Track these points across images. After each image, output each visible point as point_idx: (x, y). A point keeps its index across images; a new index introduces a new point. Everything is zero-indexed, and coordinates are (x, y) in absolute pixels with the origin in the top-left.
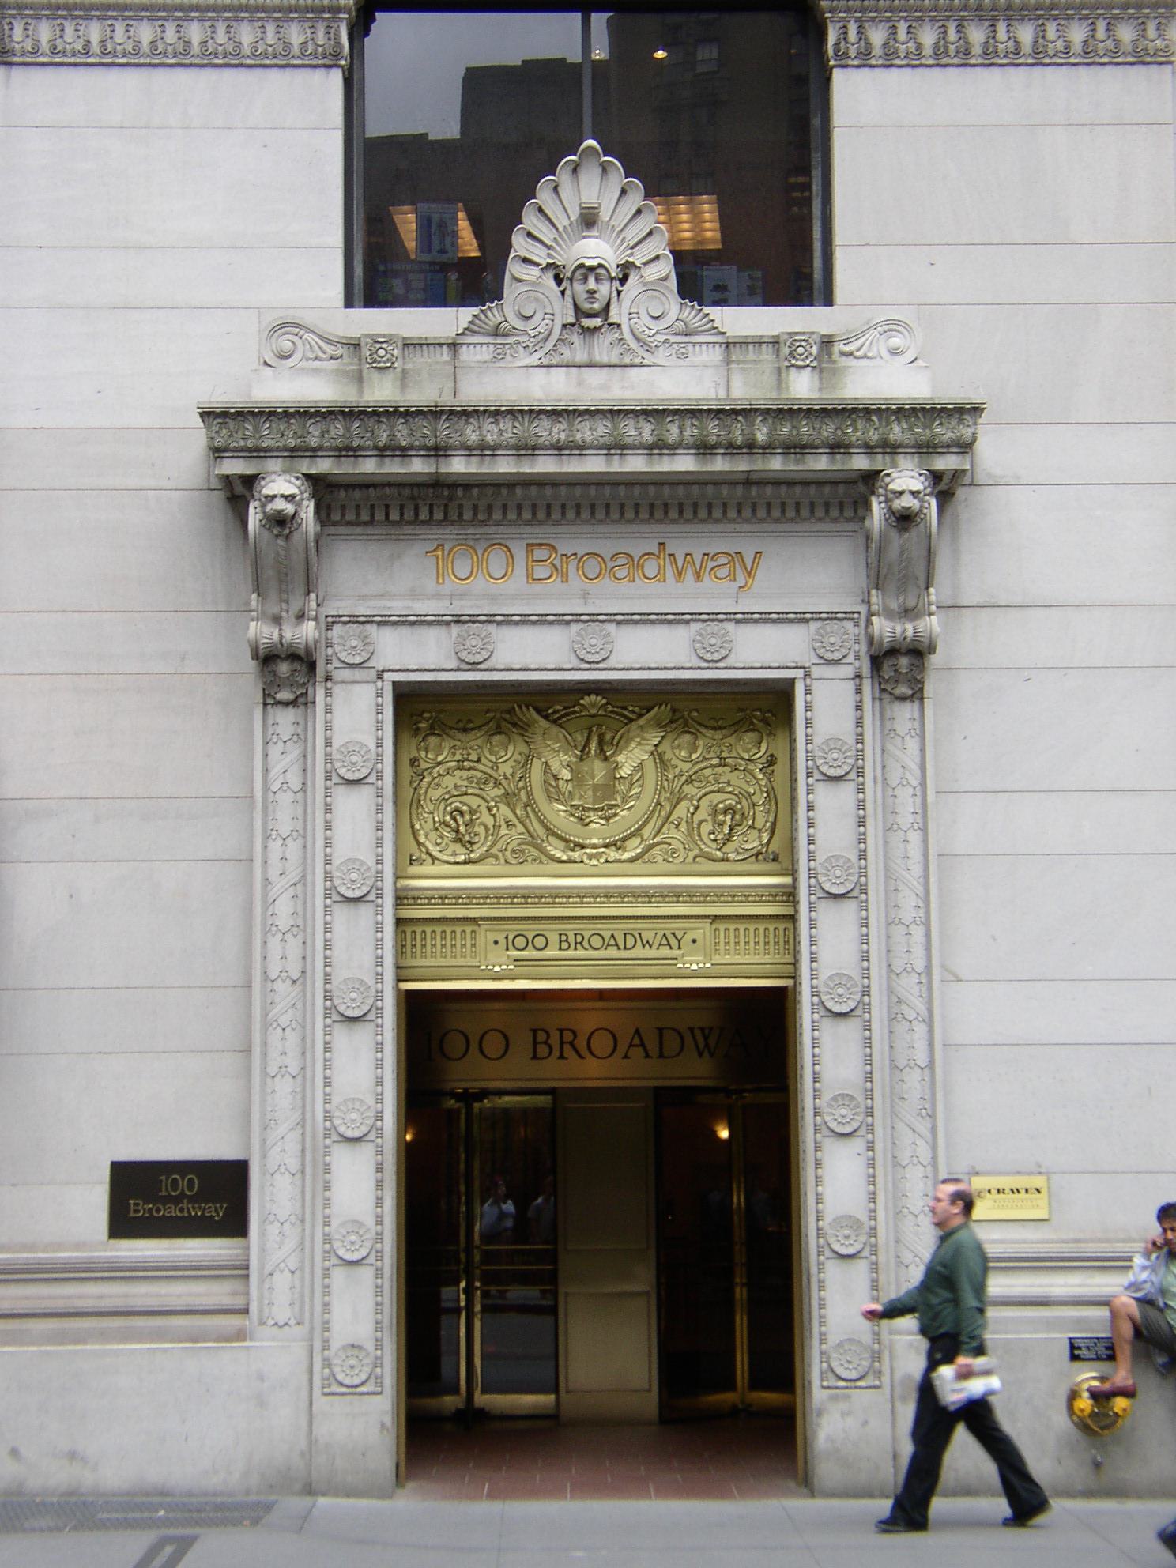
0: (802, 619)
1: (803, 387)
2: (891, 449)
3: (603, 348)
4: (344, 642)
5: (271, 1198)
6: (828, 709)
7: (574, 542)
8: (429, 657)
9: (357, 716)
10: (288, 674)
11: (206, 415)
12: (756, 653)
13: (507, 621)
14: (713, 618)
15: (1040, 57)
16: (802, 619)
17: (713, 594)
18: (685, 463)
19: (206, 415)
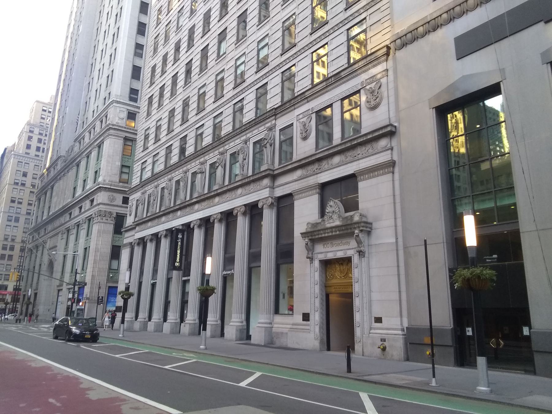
0: (352, 249)
1: (349, 222)
2: (355, 228)
3: (331, 221)
4: (315, 256)
5: (311, 317)
6: (356, 259)
7: (334, 242)
8: (322, 257)
9: (317, 263)
10: (311, 259)
11: (301, 234)
12: (349, 253)
13: (328, 252)
14: (344, 250)
15: (378, 176)
16: (352, 249)
17: (346, 247)
18: (338, 233)
19: (301, 234)
